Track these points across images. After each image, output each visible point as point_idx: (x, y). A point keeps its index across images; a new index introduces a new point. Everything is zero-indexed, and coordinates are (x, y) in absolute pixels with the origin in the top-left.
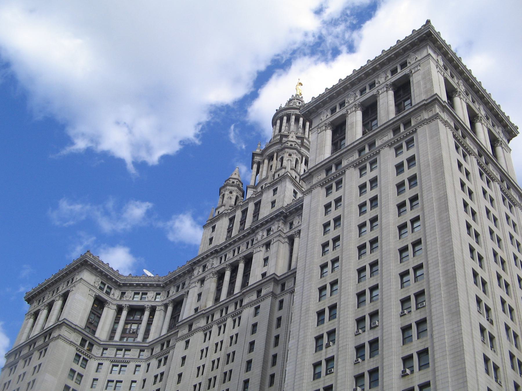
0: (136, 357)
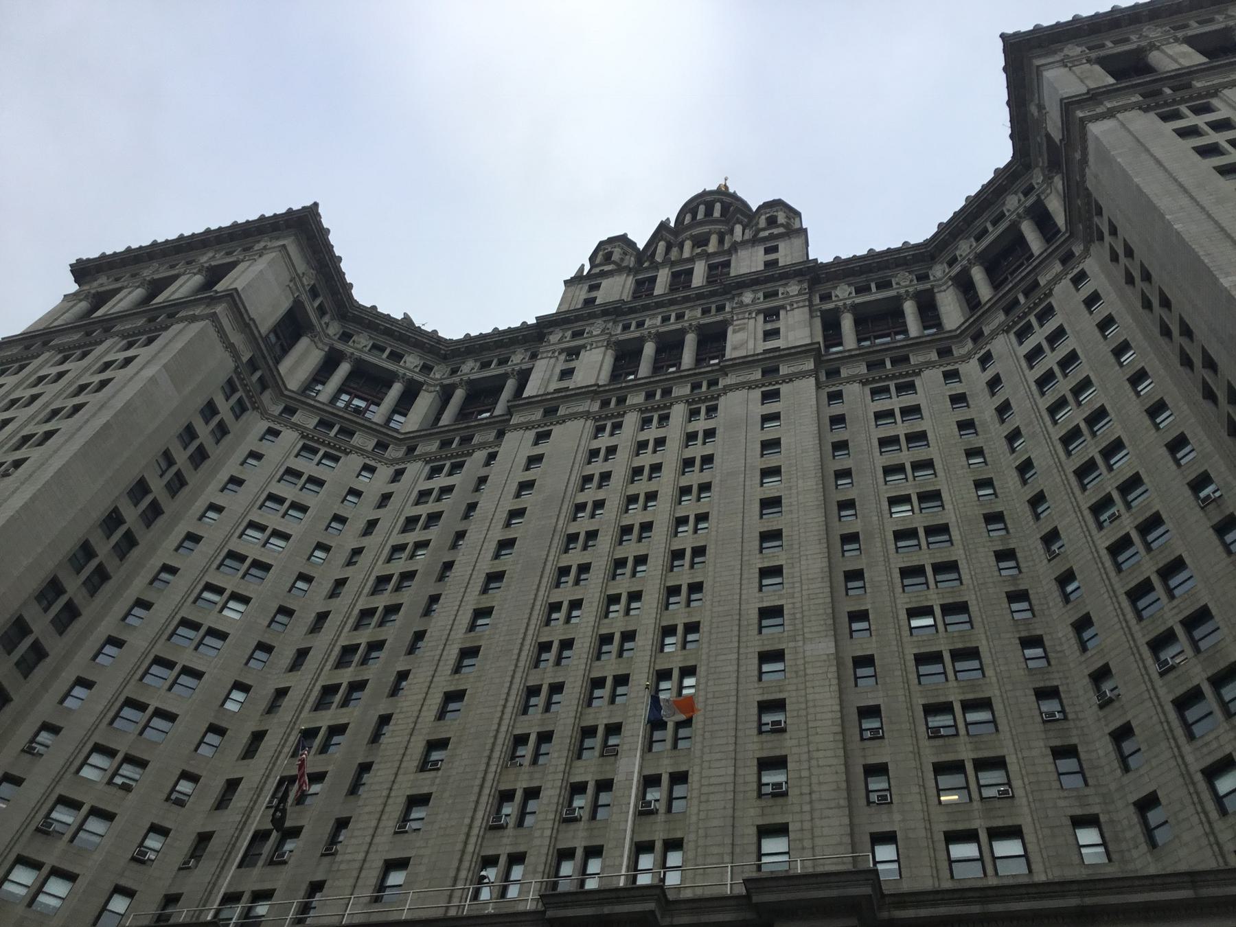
0: (370, 448)
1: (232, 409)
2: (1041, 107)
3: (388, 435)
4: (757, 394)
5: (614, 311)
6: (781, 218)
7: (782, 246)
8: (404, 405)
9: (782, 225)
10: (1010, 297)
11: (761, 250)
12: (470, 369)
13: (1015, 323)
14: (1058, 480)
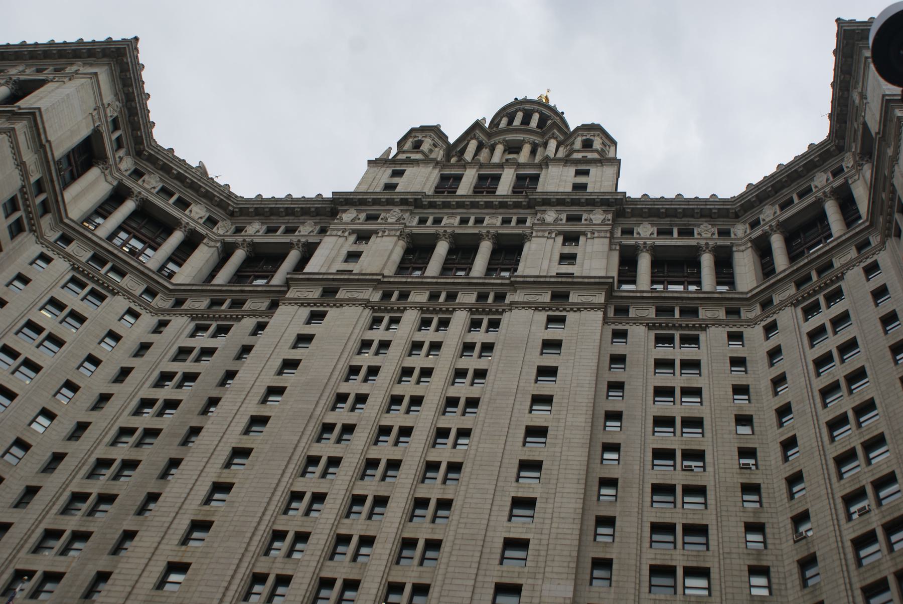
1: (10, 227)
2: (863, 96)
3: (158, 283)
4: (542, 317)
5: (414, 203)
6: (597, 144)
7: (593, 171)
8: (181, 255)
9: (596, 151)
10: (803, 273)
11: (572, 170)
12: (255, 230)
13: (804, 299)
14: (818, 463)
